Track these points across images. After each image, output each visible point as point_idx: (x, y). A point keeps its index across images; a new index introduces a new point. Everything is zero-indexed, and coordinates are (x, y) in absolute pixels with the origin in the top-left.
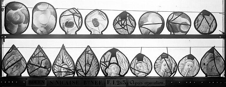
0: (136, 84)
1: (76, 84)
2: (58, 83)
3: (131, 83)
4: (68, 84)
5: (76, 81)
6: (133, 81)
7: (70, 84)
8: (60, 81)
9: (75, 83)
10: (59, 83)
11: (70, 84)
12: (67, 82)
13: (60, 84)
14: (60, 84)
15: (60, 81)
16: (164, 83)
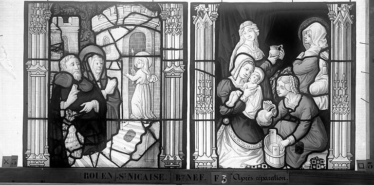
0: (242, 180)
1: (160, 179)
2: (132, 177)
3: (234, 178)
4: (147, 179)
5: (160, 175)
6: (239, 175)
7: (151, 179)
8: (135, 174)
9: (158, 178)
10: (134, 178)
11: (151, 179)
12: (145, 176)
13: (135, 179)
14: (135, 179)
15: (135, 174)
16: (287, 177)
